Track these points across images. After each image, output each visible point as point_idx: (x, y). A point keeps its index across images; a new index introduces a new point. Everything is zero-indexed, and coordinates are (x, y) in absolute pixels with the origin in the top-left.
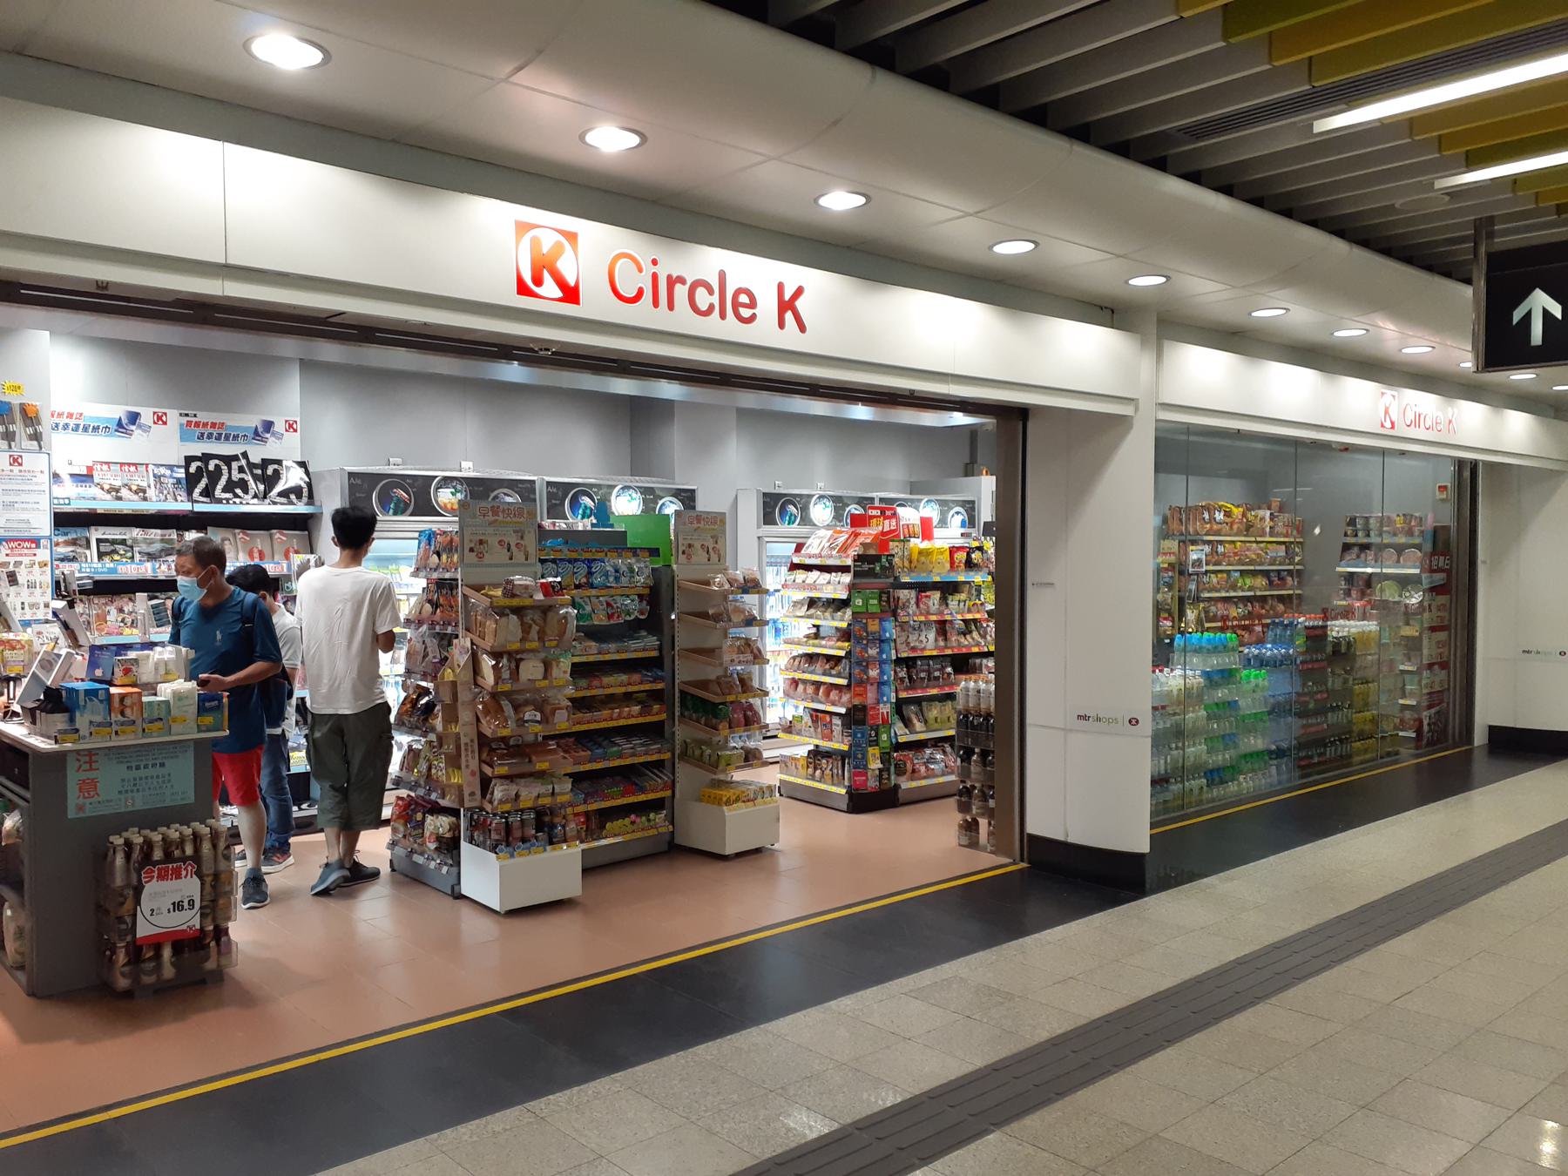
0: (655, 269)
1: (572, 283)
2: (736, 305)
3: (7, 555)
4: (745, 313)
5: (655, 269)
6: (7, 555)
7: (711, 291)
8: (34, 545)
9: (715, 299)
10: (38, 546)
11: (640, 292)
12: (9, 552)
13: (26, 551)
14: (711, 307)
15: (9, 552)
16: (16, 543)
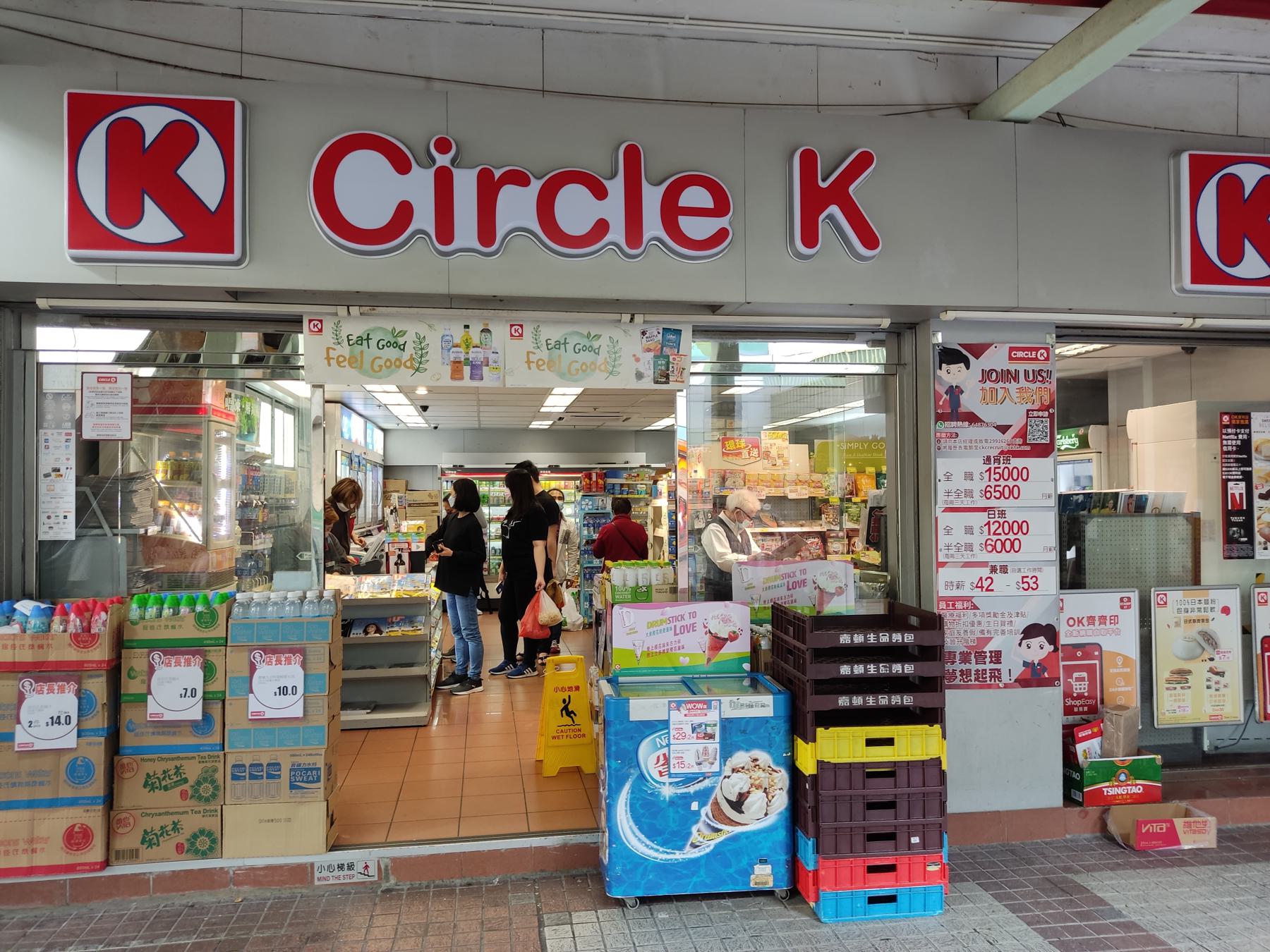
0: (443, 160)
1: (213, 207)
2: (671, 211)
3: (685, 715)
4: (696, 228)
5: (443, 160)
6: (685, 715)
7: (600, 192)
8: (705, 707)
9: (614, 208)
10: (709, 707)
11: (404, 212)
12: (686, 712)
13: (699, 712)
14: (601, 227)
15: (686, 712)
16: (692, 705)
